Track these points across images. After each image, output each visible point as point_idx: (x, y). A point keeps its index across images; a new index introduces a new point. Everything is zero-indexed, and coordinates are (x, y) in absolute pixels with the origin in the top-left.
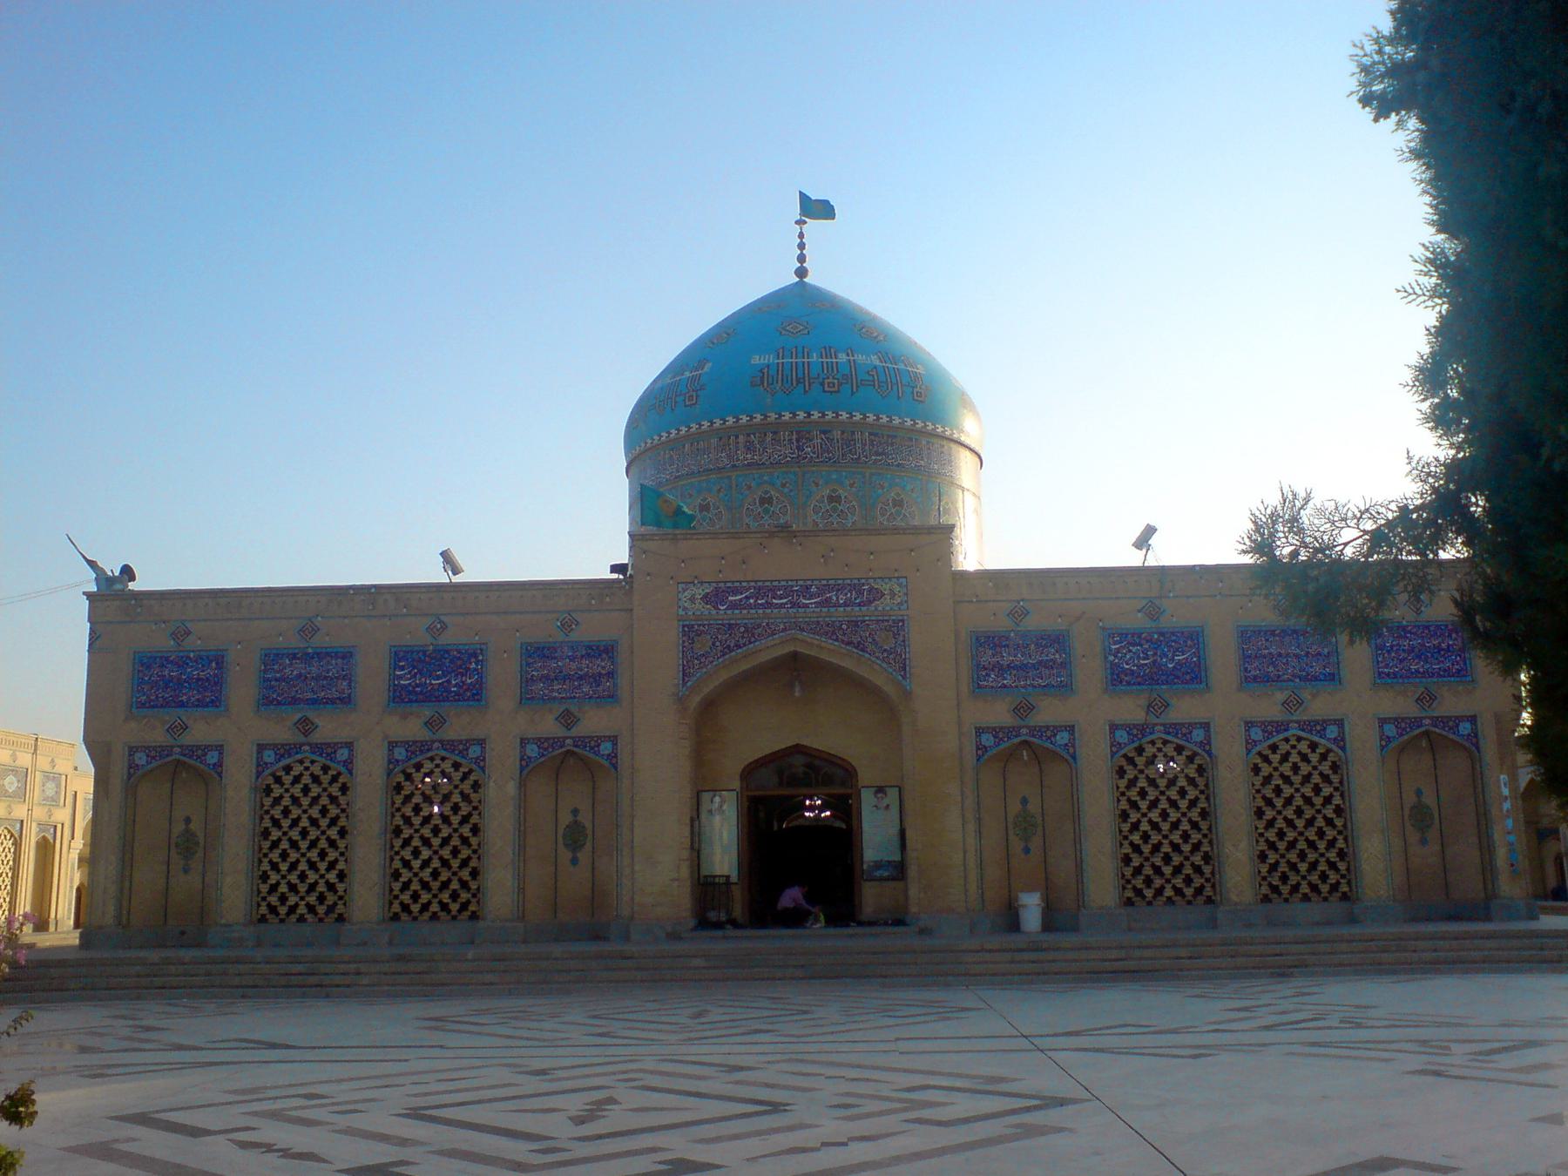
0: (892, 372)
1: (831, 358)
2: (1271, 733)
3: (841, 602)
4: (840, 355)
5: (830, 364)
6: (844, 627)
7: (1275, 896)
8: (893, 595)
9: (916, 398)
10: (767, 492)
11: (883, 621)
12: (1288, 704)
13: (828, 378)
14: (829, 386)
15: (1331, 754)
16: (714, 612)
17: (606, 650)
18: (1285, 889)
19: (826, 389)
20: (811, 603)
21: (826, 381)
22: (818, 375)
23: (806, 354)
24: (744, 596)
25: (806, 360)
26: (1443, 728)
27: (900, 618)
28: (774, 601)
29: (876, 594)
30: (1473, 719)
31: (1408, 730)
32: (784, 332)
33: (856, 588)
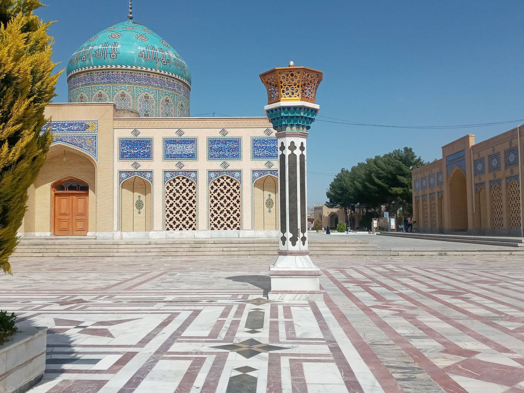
0: (155, 53)
2: (261, 175)
3: (75, 129)
6: (76, 138)
7: (184, 228)
8: (93, 127)
10: (100, 93)
11: (88, 136)
13: (113, 53)
15: (237, 183)
26: (274, 174)
27: (94, 135)
28: (53, 128)
29: (87, 127)
31: (263, 175)
32: (111, 37)
33: (81, 124)
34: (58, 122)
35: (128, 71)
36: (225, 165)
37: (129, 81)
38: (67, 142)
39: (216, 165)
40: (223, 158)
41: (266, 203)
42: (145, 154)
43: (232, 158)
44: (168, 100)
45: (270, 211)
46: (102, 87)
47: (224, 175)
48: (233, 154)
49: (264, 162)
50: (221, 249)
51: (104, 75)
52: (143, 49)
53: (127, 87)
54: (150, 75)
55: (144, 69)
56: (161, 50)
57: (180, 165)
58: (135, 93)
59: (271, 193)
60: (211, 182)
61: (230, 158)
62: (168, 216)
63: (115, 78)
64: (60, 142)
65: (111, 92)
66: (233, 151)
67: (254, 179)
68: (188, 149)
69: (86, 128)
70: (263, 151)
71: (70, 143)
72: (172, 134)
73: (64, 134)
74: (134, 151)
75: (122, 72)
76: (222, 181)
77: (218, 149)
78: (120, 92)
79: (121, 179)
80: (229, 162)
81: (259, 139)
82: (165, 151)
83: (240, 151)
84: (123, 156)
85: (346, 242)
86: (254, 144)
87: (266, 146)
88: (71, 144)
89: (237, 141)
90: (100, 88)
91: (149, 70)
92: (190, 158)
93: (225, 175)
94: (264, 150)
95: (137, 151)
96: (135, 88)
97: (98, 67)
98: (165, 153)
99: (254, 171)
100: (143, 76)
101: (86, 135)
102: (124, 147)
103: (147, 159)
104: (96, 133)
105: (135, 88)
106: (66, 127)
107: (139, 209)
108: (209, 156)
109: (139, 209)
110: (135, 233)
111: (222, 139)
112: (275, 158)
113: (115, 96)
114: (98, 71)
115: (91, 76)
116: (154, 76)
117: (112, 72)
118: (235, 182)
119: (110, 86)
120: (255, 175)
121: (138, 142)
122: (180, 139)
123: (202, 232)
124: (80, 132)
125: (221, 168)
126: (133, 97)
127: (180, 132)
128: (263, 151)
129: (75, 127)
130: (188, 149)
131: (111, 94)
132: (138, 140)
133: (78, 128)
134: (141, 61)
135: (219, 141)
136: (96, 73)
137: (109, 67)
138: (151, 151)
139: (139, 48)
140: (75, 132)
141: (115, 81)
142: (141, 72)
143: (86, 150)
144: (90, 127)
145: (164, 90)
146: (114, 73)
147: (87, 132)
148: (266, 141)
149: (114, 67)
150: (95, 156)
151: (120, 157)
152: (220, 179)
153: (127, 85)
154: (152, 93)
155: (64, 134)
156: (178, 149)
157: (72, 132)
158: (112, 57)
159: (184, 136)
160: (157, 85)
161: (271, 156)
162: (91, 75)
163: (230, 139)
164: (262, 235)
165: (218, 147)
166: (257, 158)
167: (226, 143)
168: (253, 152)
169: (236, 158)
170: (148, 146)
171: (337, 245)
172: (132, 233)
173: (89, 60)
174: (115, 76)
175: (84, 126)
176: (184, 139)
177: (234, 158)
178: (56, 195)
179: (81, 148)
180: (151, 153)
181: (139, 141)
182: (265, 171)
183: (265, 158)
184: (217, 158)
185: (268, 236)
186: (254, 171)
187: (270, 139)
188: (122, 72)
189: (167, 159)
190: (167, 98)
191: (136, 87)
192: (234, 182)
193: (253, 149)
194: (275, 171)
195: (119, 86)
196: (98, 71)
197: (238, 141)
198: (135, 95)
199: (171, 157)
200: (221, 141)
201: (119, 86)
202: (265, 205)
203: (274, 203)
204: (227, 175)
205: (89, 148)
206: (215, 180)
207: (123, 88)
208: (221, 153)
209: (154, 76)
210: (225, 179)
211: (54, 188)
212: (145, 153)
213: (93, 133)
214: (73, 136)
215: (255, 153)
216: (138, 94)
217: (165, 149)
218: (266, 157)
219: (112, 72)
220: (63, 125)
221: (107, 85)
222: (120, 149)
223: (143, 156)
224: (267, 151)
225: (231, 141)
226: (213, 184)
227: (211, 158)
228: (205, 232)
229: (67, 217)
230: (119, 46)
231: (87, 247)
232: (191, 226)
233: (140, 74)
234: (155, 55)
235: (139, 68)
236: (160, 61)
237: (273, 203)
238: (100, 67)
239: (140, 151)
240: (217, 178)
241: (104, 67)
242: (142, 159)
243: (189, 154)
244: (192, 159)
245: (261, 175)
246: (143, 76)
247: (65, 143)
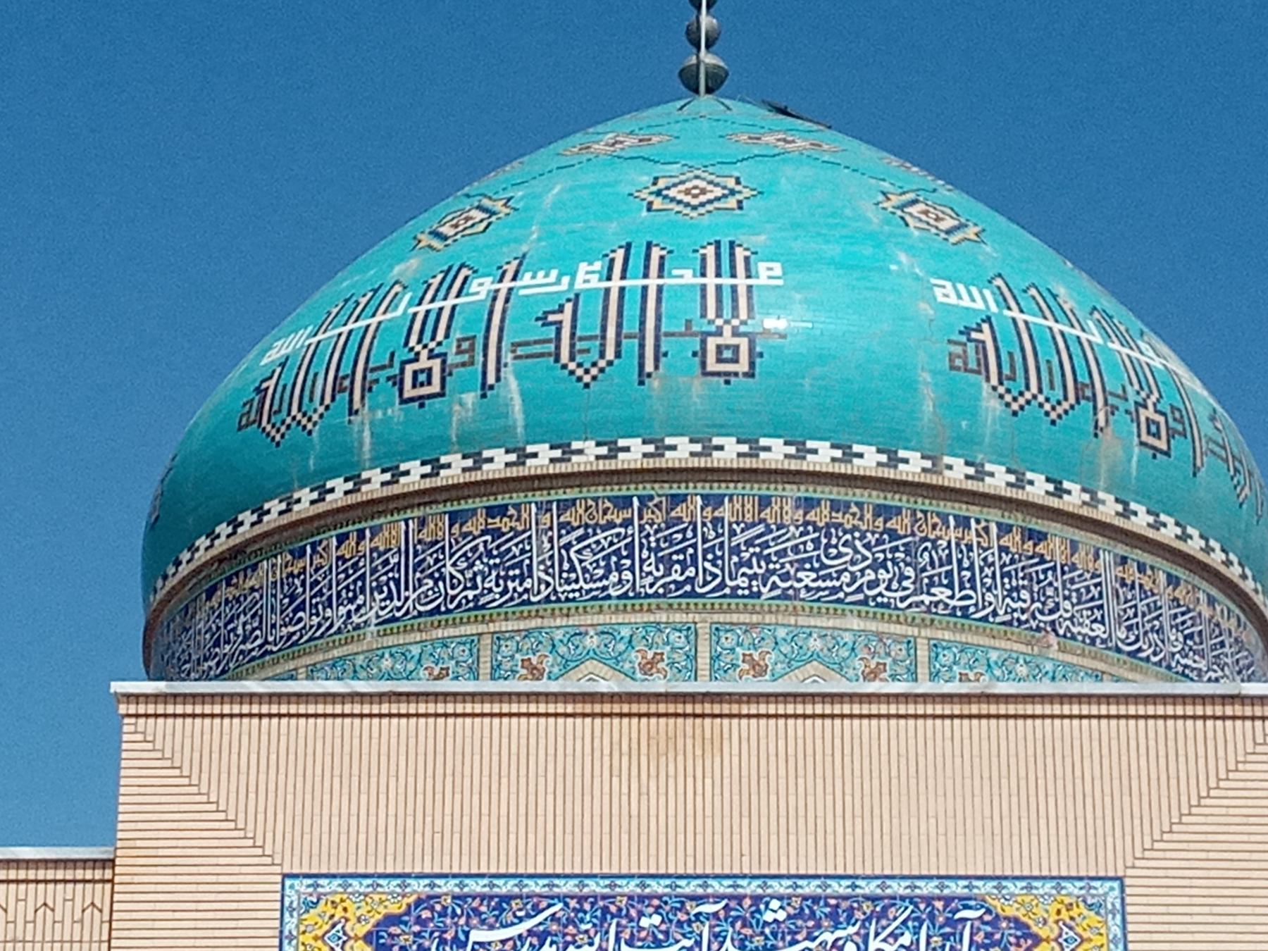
25: (726, 281)
35: (860, 495)
37: (873, 584)
46: (607, 632)
51: (627, 523)
52: (980, 305)
53: (848, 637)
55: (998, 481)
63: (736, 551)
75: (809, 504)
90: (591, 642)
91: (1038, 489)
96: (923, 653)
97: (568, 452)
105: (923, 653)
114: (571, 494)
115: (497, 533)
116: (1074, 546)
117: (713, 501)
134: (973, 413)
137: (682, 452)
139: (945, 293)
142: (973, 511)
146: (726, 512)
149: (729, 452)
153: (856, 624)
158: (712, 366)
160: (1099, 630)
162: (496, 522)
188: (809, 504)
191: (935, 646)
195: (781, 633)
196: (571, 494)
201: (781, 633)
207: (815, 644)
209: (1074, 546)
219: (713, 501)
230: (767, 273)
233: (963, 523)
234: (1079, 361)
235: (957, 473)
238: (588, 455)
241: (635, 453)
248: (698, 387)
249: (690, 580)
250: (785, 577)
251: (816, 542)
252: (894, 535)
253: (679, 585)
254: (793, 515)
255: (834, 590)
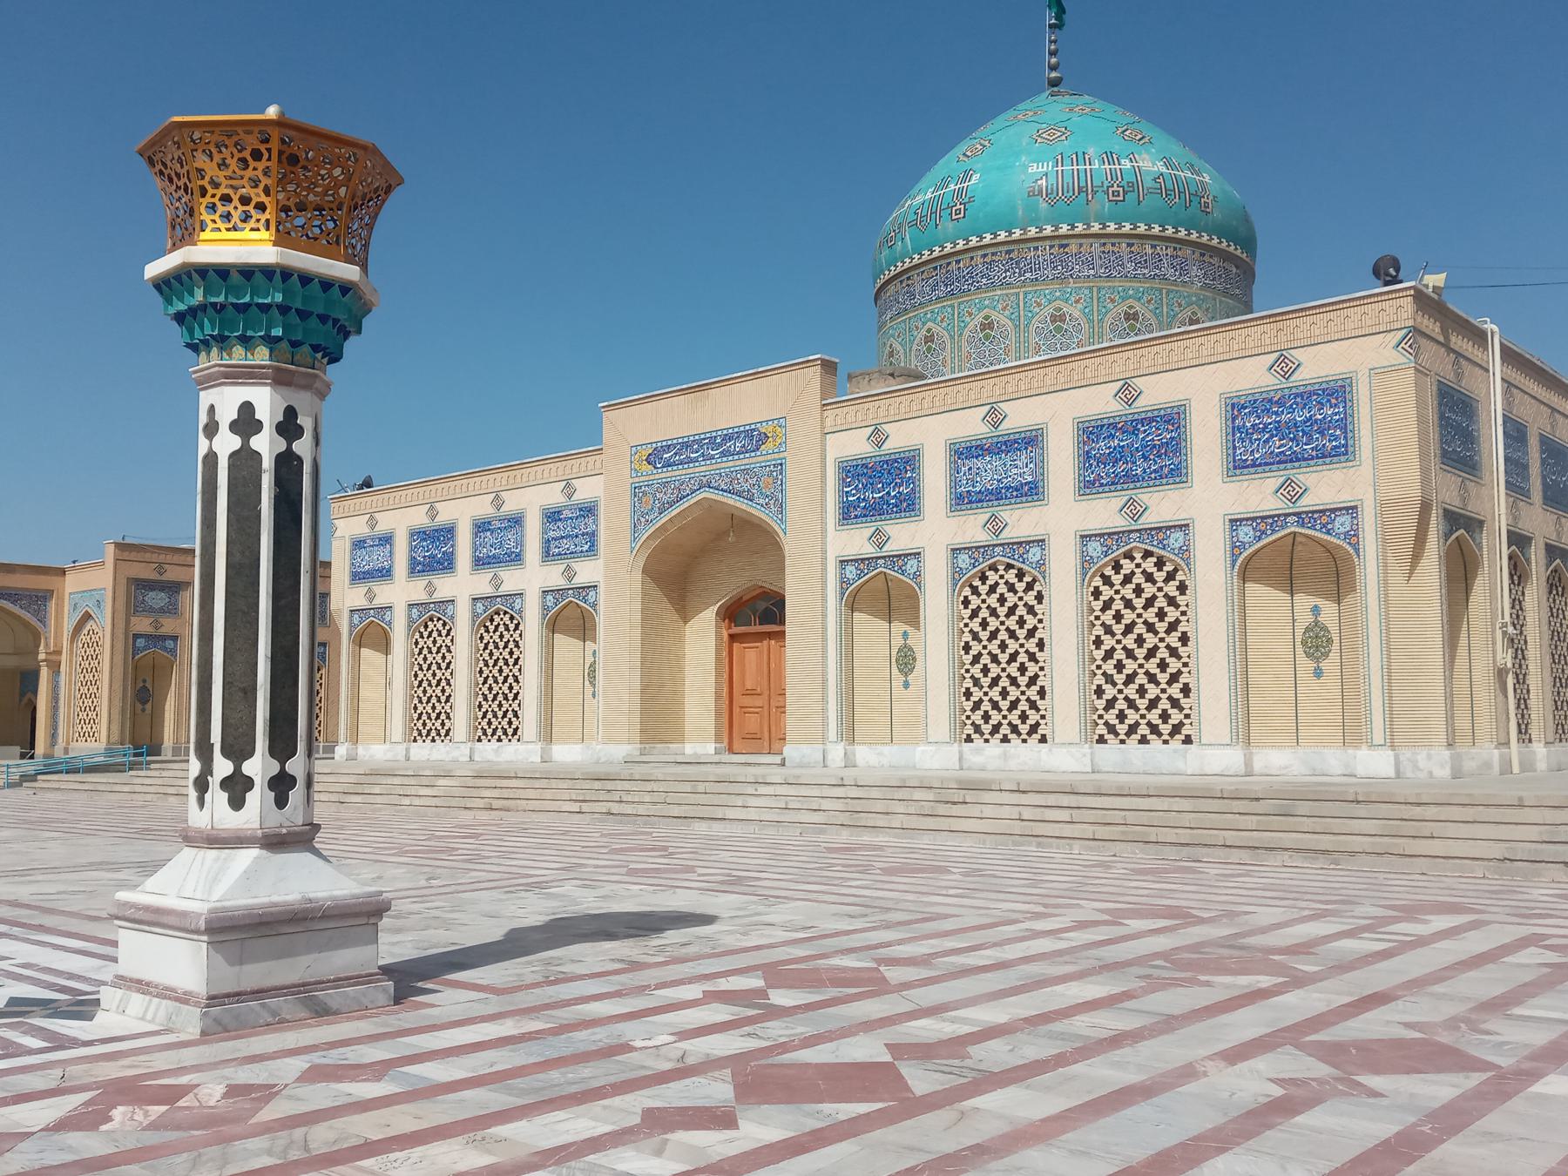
1: (1114, 164)
4: (1122, 161)
5: (1113, 170)
9: (962, 215)
12: (1135, 515)
14: (1113, 195)
16: (655, 472)
17: (589, 510)
18: (1122, 729)
19: (1122, 199)
20: (717, 454)
21: (1111, 190)
22: (1102, 183)
23: (1116, 160)
24: (672, 453)
26: (1313, 528)
28: (692, 455)
30: (1352, 510)
33: (749, 434)
34: (702, 436)
35: (1001, 248)
36: (1133, 509)
38: (722, 490)
39: (1105, 512)
40: (1125, 486)
41: (1304, 643)
42: (901, 501)
43: (1158, 482)
44: (1136, 314)
45: (1318, 673)
47: (1131, 545)
48: (1161, 467)
49: (1272, 481)
50: (1014, 812)
51: (937, 275)
54: (1067, 245)
55: (1048, 230)
56: (1109, 157)
57: (996, 525)
58: (1022, 313)
59: (1320, 602)
60: (1090, 574)
61: (1151, 483)
62: (968, 694)
63: (964, 277)
64: (707, 489)
65: (956, 322)
66: (1160, 456)
67: (1237, 551)
68: (1018, 469)
69: (761, 443)
70: (1267, 441)
71: (726, 491)
72: (972, 425)
73: (715, 467)
74: (875, 495)
76: (1127, 566)
77: (1109, 454)
78: (979, 318)
79: (844, 582)
80: (1145, 497)
81: (1250, 398)
82: (954, 483)
83: (1183, 451)
84: (848, 514)
85: (1521, 799)
86: (1233, 420)
87: (1279, 422)
88: (730, 492)
89: (1173, 419)
92: (1024, 499)
93: (1134, 544)
94: (1272, 436)
95: (880, 495)
98: (953, 490)
99: (1236, 520)
100: (1045, 252)
101: (761, 462)
102: (849, 486)
103: (908, 514)
104: (781, 455)
106: (720, 445)
107: (906, 676)
108: (1082, 485)
109: (906, 676)
110: (895, 747)
111: (1124, 418)
112: (1312, 463)
113: (966, 333)
118: (1171, 568)
119: (952, 306)
120: (1241, 535)
121: (885, 466)
122: (995, 440)
123: (1065, 750)
124: (747, 455)
125: (1120, 523)
126: (1016, 326)
127: (994, 416)
128: (1267, 441)
129: (737, 444)
130: (1018, 469)
131: (956, 329)
132: (883, 458)
133: (744, 445)
135: (1114, 425)
136: (918, 275)
137: (949, 248)
138: (917, 489)
140: (736, 457)
141: (966, 287)
142: (1040, 243)
143: (762, 506)
144: (768, 438)
145: (1117, 284)
146: (961, 265)
147: (764, 452)
148: (1276, 402)
149: (961, 245)
150: (781, 520)
151: (841, 517)
152: (1122, 562)
153: (999, 292)
154: (1077, 302)
155: (715, 467)
156: (990, 471)
157: (730, 458)
159: (1006, 426)
160: (1092, 272)
161: (1296, 459)
163: (1150, 415)
164: (1286, 768)
165: (1110, 448)
166: (1246, 471)
167: (1135, 432)
168: (1230, 451)
169: (1171, 481)
170: (909, 474)
171: (1469, 814)
172: (886, 749)
173: (903, 239)
174: (965, 273)
175: (754, 438)
176: (1006, 438)
177: (1164, 481)
178: (732, 637)
179: (750, 503)
180: (917, 495)
181: (887, 462)
182: (1278, 516)
183: (1274, 467)
184: (1107, 489)
185: (1314, 770)
186: (1235, 523)
187: (1294, 391)
188: (985, 256)
189: (959, 508)
190: (1131, 307)
192: (1169, 567)
193: (1230, 438)
194: (1316, 516)
197: (1176, 416)
198: (1022, 319)
199: (970, 502)
200: (1120, 426)
201: (977, 301)
202: (1300, 650)
203: (1336, 639)
204: (1144, 546)
205: (767, 500)
206: (1105, 565)
207: (987, 302)
208: (1121, 468)
210: (1138, 560)
211: (727, 621)
212: (900, 498)
213: (776, 456)
214: (732, 469)
215: (1238, 452)
216: (1030, 315)
217: (953, 478)
218: (1279, 462)
219: (958, 262)
220: (712, 440)
221: (945, 304)
222: (841, 494)
223: (897, 506)
224: (1280, 440)
225: (1152, 420)
226: (1098, 582)
227: (1088, 491)
228: (1073, 749)
229: (758, 701)
231: (688, 787)
232: (1176, 729)
235: (1032, 232)
236: (1100, 195)
237: (1330, 641)
239: (888, 493)
240: (1110, 557)
242: (893, 516)
243: (1022, 484)
244: (1030, 499)
245: (1263, 532)
246: (1045, 252)
247: (716, 492)
248: (951, 225)
249: (952, 290)
250: (977, 283)
251: (987, 268)
252: (1012, 259)
253: (949, 292)
254: (980, 260)
255: (992, 283)
